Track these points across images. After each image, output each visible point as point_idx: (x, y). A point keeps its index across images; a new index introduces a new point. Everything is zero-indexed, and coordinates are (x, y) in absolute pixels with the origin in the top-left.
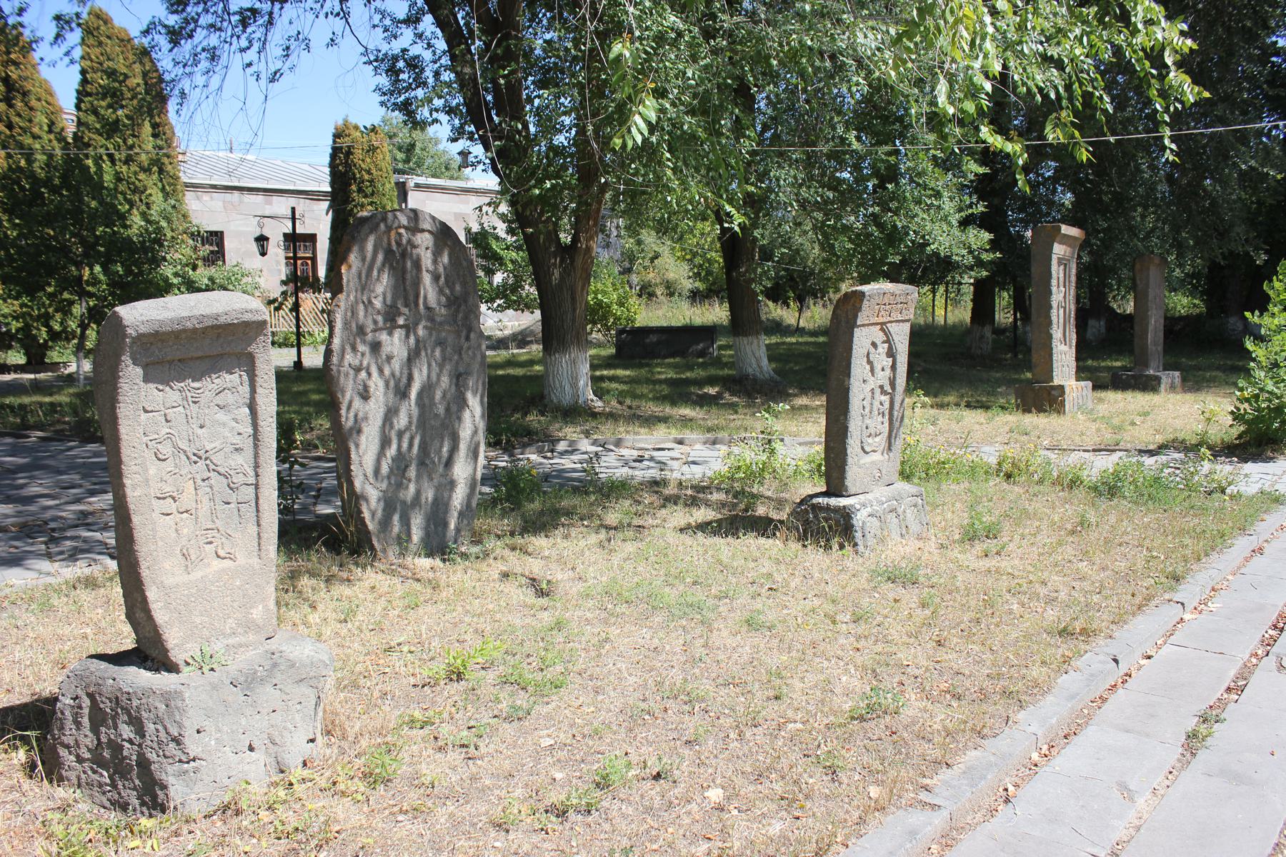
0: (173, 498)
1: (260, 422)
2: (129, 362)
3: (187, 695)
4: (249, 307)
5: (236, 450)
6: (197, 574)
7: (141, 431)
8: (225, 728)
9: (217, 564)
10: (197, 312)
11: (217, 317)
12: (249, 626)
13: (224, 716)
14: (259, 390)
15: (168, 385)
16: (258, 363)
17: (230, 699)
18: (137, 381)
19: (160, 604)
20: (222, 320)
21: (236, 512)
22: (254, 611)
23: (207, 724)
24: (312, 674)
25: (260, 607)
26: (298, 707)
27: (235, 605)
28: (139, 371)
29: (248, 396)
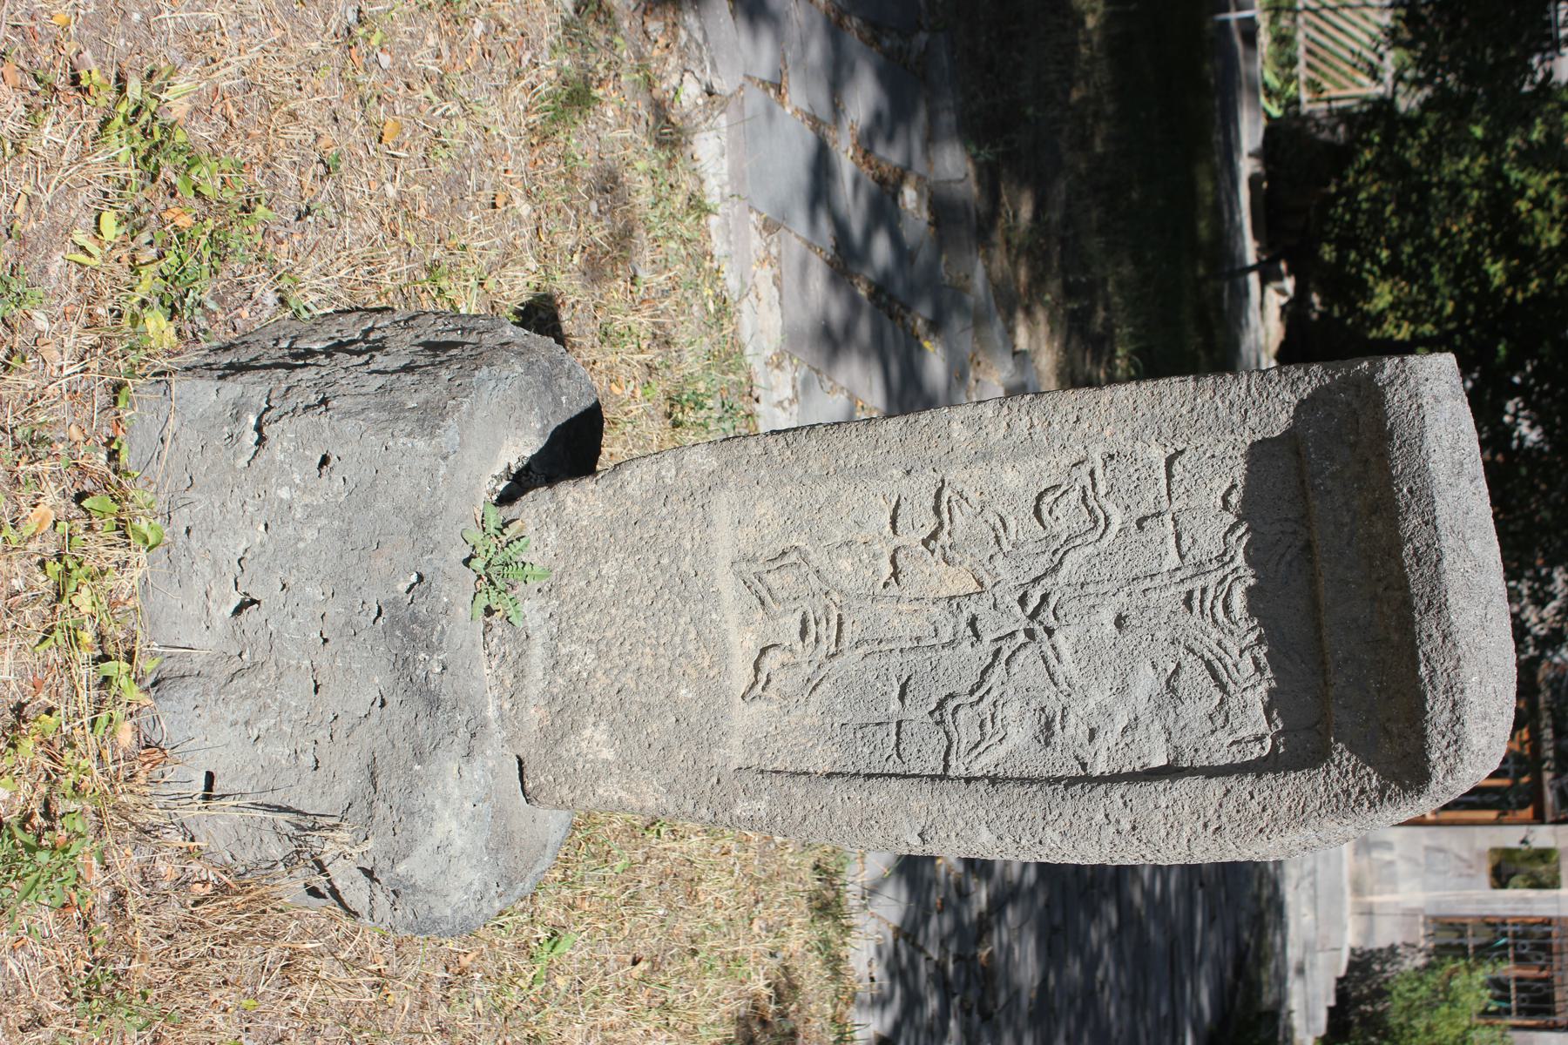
0: (934, 536)
1: (1118, 791)
2: (1305, 389)
3: (421, 444)
4: (1470, 715)
5: (1049, 725)
6: (727, 585)
7: (1122, 442)
8: (310, 534)
9: (744, 645)
10: (1448, 543)
11: (1438, 607)
12: (566, 713)
13: (345, 535)
14: (1216, 786)
15: (1241, 519)
16: (1294, 782)
17: (381, 563)
18: (1253, 421)
19: (669, 475)
20: (1427, 625)
21: (876, 716)
22: (601, 735)
23: (334, 484)
24: (382, 808)
25: (608, 754)
26: (308, 760)
27: (628, 679)
28: (1282, 421)
29: (1202, 760)
